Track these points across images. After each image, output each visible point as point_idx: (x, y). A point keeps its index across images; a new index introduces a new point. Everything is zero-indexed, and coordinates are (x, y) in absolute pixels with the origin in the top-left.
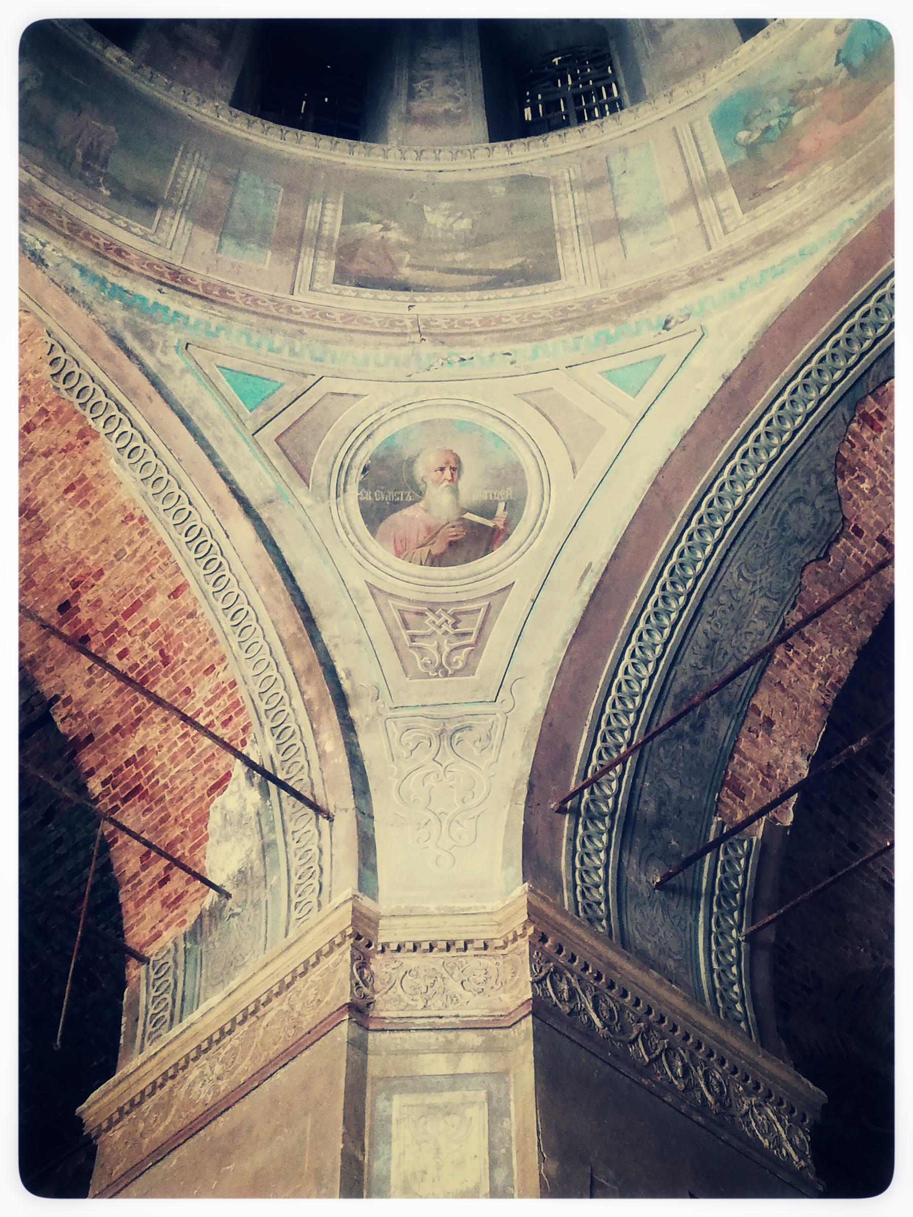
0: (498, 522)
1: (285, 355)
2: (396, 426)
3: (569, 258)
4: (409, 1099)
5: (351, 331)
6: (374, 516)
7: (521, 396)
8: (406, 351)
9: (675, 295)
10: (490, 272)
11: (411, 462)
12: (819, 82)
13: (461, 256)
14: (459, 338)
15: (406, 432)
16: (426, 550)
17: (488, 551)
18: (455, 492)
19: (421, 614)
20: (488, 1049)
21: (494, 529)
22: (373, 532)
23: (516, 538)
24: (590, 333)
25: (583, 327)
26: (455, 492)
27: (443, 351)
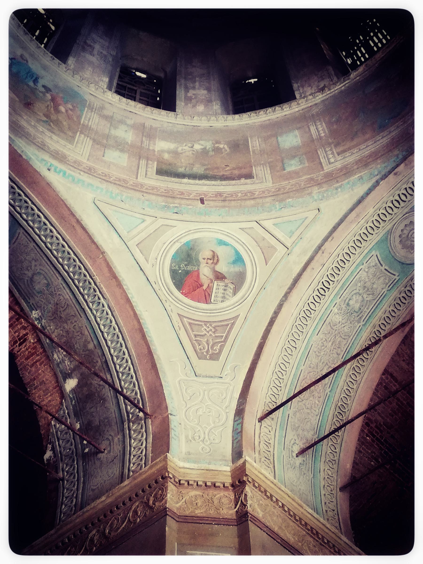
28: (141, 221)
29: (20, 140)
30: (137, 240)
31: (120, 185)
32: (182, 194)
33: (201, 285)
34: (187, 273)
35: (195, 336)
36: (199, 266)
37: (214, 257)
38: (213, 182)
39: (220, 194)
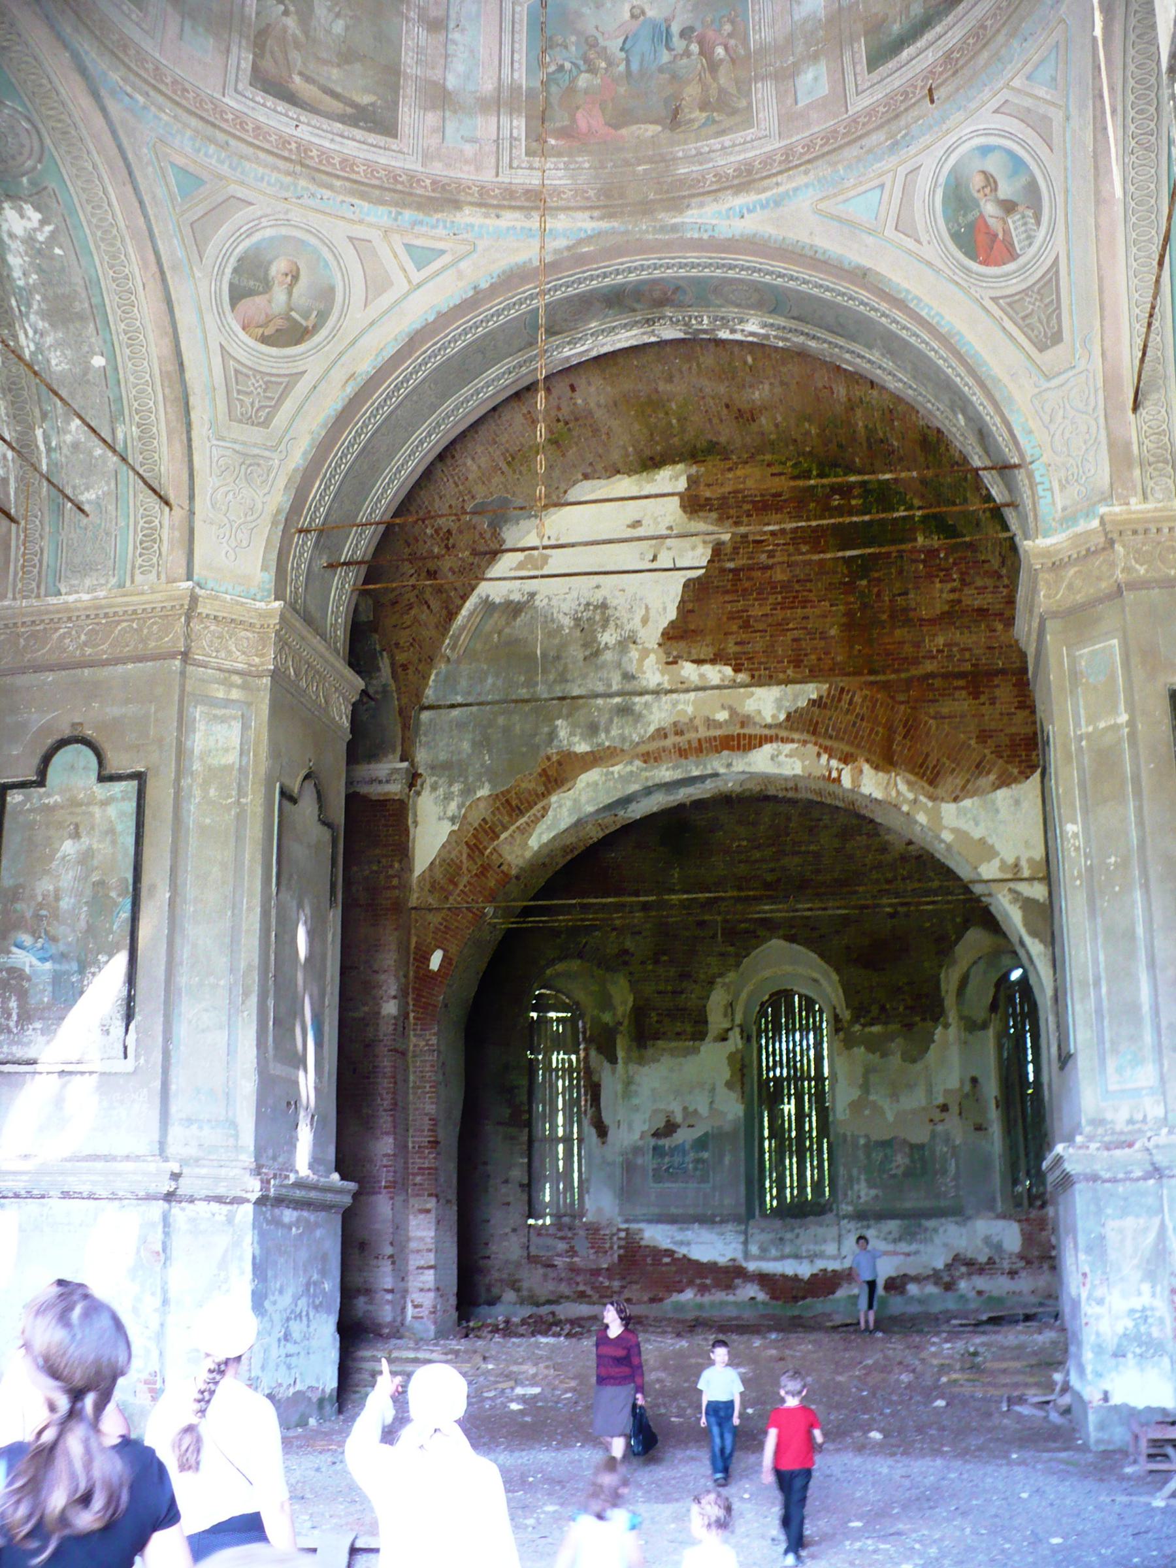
0: (309, 324)
1: (214, 161)
2: (269, 233)
3: (408, 115)
4: (205, 709)
5: (259, 147)
6: (237, 295)
7: (350, 239)
8: (289, 179)
9: (467, 210)
10: (354, 105)
11: (270, 263)
12: (603, 53)
13: (335, 73)
14: (324, 177)
15: (272, 239)
16: (260, 331)
17: (298, 342)
18: (290, 294)
19: (247, 376)
20: (244, 687)
21: (306, 328)
22: (233, 305)
23: (317, 339)
24: (408, 215)
25: (404, 205)
26: (290, 294)
27: (313, 188)
28: (878, 191)
29: (690, 212)
30: (891, 223)
31: (828, 153)
32: (906, 93)
33: (996, 236)
34: (971, 227)
35: (1024, 318)
36: (978, 206)
37: (987, 179)
38: (939, 29)
39: (948, 57)
